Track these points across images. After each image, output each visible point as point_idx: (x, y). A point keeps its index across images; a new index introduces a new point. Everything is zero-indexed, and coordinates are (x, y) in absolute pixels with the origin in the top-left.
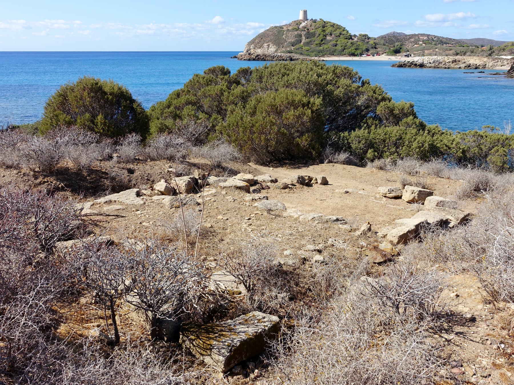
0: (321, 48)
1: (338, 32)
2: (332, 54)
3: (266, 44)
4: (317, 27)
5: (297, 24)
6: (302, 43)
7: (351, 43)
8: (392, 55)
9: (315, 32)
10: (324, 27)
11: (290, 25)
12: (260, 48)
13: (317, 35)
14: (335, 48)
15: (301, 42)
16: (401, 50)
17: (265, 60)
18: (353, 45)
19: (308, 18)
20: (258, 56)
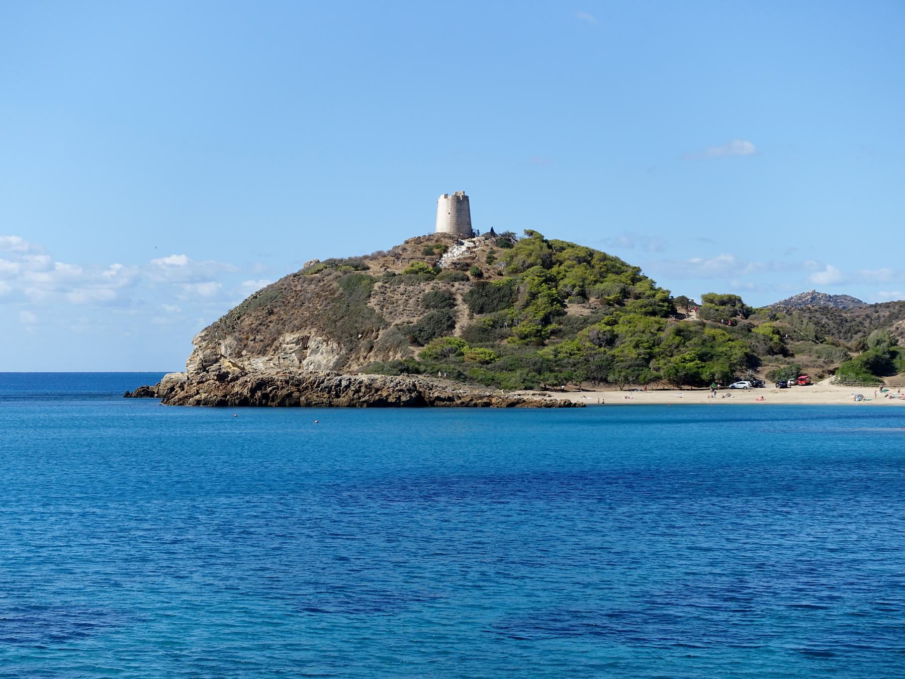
0: (547, 351)
1: (611, 285)
2: (600, 377)
3: (289, 337)
4: (517, 262)
5: (429, 252)
6: (457, 332)
7: (678, 332)
8: (864, 383)
9: (510, 283)
10: (548, 264)
11: (397, 257)
12: (263, 352)
13: (523, 298)
14: (610, 352)
15: (452, 327)
16: (897, 362)
17: (297, 404)
18: (687, 338)
19: (475, 227)
20: (261, 384)
